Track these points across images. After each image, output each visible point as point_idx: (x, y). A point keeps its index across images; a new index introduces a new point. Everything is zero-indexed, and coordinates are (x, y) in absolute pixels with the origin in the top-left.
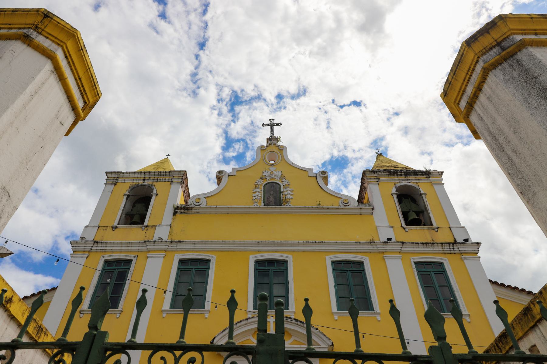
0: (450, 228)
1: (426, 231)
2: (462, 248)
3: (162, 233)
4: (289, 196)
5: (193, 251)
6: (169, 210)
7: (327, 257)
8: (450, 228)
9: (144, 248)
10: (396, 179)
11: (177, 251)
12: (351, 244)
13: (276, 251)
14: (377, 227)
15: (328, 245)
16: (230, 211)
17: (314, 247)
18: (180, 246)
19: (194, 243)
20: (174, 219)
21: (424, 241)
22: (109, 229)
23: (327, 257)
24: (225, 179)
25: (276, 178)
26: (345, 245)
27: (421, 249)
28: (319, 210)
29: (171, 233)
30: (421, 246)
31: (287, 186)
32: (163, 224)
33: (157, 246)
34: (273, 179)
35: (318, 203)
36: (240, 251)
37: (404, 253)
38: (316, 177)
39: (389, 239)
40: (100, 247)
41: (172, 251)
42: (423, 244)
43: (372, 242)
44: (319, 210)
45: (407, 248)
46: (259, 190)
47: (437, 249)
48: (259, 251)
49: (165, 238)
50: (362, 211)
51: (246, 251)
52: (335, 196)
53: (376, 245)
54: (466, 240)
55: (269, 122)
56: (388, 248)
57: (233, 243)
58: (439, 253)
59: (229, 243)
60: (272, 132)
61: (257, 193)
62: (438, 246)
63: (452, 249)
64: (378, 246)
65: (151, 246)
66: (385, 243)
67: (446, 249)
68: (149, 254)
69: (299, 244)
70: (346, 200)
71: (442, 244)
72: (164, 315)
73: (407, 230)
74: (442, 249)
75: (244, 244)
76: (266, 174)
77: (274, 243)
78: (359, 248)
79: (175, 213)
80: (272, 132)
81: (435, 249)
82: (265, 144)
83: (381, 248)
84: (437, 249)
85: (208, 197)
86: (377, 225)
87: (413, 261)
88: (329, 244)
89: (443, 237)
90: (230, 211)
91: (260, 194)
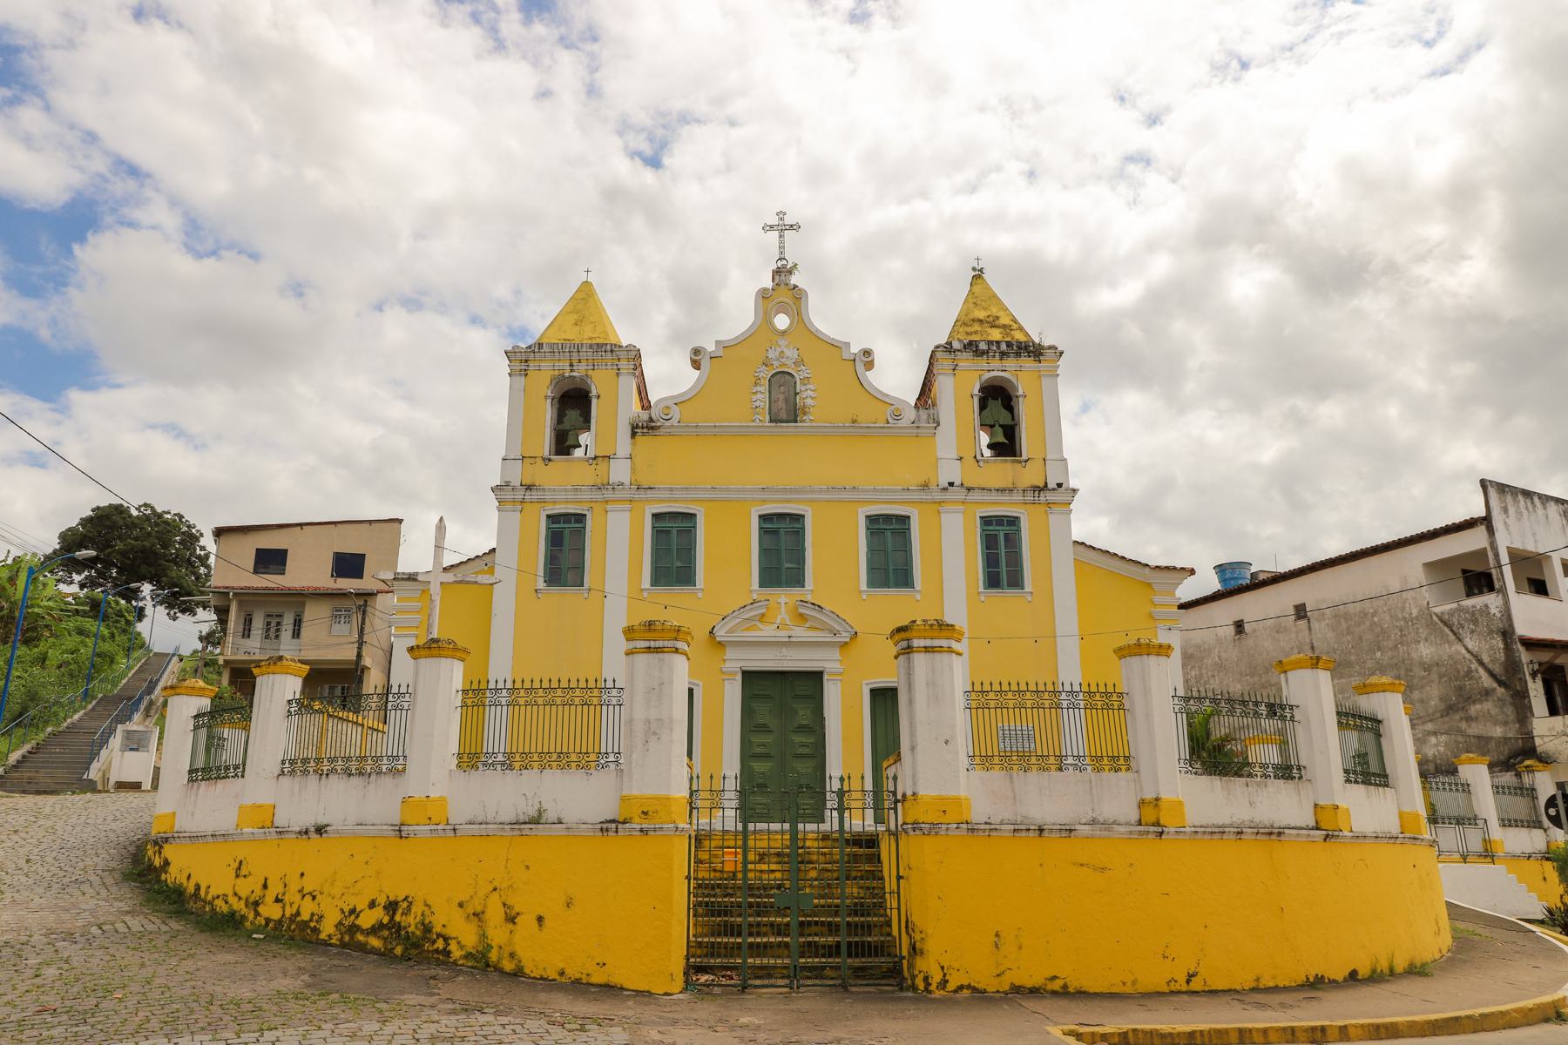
1: (1009, 465)
2: (1051, 497)
3: (620, 472)
4: (809, 402)
5: (669, 500)
6: (624, 431)
9: (597, 496)
11: (647, 500)
13: (788, 501)
16: (717, 432)
17: (843, 496)
18: (650, 494)
19: (671, 490)
20: (634, 444)
22: (539, 461)
24: (705, 363)
25: (789, 362)
27: (994, 497)
28: (855, 429)
29: (633, 470)
31: (805, 381)
32: (619, 454)
33: (618, 495)
34: (784, 365)
36: (738, 500)
39: (951, 484)
40: (535, 495)
41: (641, 500)
43: (925, 486)
44: (855, 429)
45: (975, 496)
46: (761, 389)
48: (764, 501)
49: (627, 481)
51: (745, 500)
52: (881, 400)
54: (1060, 485)
55: (774, 221)
57: (728, 490)
59: (721, 490)
60: (782, 247)
61: (759, 396)
65: (609, 495)
66: (945, 489)
67: (1029, 497)
68: (609, 507)
69: (821, 491)
72: (645, 594)
75: (743, 491)
76: (771, 355)
77: (785, 490)
79: (634, 434)
80: (782, 247)
82: (769, 284)
83: (938, 496)
85: (680, 402)
86: (939, 455)
88: (864, 491)
90: (717, 432)
91: (762, 399)
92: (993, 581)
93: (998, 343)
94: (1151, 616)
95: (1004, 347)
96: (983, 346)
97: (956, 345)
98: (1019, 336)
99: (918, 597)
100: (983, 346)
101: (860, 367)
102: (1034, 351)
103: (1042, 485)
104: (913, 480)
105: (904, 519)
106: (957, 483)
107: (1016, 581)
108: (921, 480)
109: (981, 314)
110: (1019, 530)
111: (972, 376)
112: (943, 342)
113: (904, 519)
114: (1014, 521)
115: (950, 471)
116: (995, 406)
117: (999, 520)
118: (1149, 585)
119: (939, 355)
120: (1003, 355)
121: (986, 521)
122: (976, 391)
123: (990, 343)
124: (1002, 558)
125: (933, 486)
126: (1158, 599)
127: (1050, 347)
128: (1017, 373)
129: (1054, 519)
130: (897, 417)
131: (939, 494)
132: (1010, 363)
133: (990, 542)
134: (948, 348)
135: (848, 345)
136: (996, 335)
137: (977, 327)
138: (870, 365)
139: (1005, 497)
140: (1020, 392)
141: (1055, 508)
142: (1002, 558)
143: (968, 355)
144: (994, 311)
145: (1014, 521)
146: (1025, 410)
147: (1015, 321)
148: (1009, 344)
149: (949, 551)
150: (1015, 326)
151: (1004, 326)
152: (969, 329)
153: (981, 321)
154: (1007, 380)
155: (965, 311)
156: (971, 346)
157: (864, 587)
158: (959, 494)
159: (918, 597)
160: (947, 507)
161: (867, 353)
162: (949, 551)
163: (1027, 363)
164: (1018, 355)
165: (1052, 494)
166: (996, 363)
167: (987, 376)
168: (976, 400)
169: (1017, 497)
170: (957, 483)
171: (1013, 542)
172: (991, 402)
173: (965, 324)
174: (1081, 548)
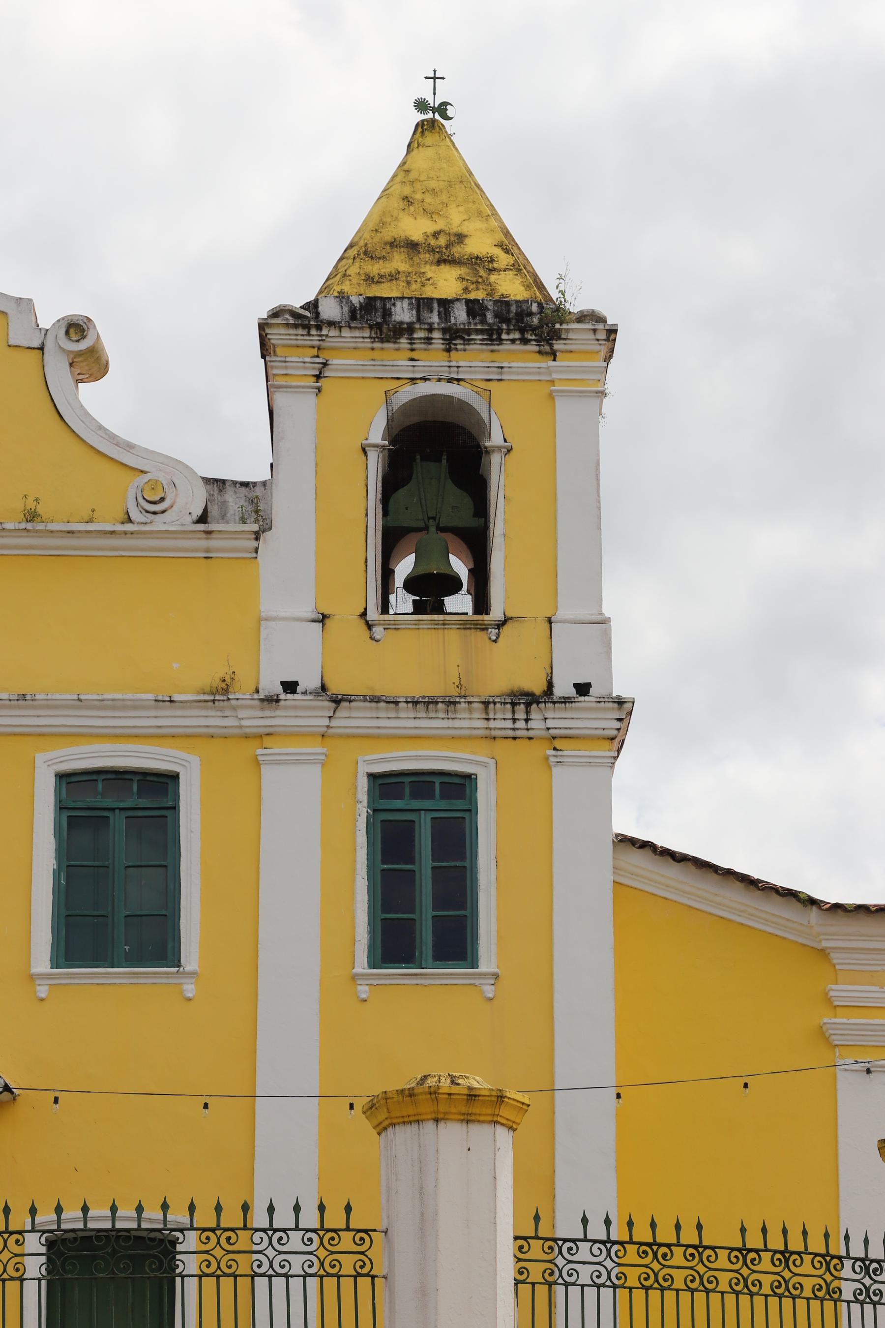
0: (550, 622)
2: (556, 719)
7: (40, 758)
8: (550, 622)
10: (397, 358)
12: (136, 706)
14: (260, 620)
15: (48, 707)
21: (417, 694)
23: (40, 758)
26: (113, 708)
27: (408, 721)
30: (406, 711)
35: (31, 504)
37: (341, 736)
38: (41, 348)
39: (290, 687)
42: (415, 703)
43: (221, 693)
45: (353, 719)
47: (465, 724)
50: (213, 543)
53: (234, 708)
54: (583, 689)
56: (279, 719)
58: (470, 738)
62: (470, 711)
63: (521, 724)
64: (241, 714)
67: (501, 722)
70: (154, 484)
71: (486, 704)
73: (378, 631)
74: (482, 724)
78: (169, 720)
81: (457, 724)
83: (253, 719)
84: (465, 724)
87: (364, 769)
88: (51, 705)
89: (509, 665)
92: (394, 945)
93: (445, 304)
94: (822, 1035)
95: (460, 315)
96: (403, 314)
97: (330, 310)
98: (511, 287)
99: (190, 989)
100: (403, 314)
101: (58, 370)
102: (536, 324)
103: (537, 687)
104: (191, 675)
105: (163, 784)
106: (309, 681)
107: (456, 944)
108: (211, 676)
109: (416, 228)
110: (472, 810)
111: (369, 395)
112: (297, 302)
113: (163, 784)
114: (460, 786)
115: (293, 653)
116: (432, 482)
117: (421, 783)
118: (823, 953)
119: (276, 335)
120: (454, 337)
121: (384, 785)
122: (377, 435)
123: (422, 304)
124: (422, 880)
125: (242, 693)
126: (841, 991)
127: (582, 317)
128: (499, 389)
129: (568, 780)
130: (156, 504)
131: (255, 711)
132: (473, 360)
133: (391, 843)
134: (306, 319)
135: (25, 305)
136: (446, 283)
137: (399, 262)
138: (91, 364)
139: (437, 722)
140: (496, 439)
141: (570, 751)
142: (422, 880)
143: (357, 336)
144: (455, 218)
145: (460, 786)
146: (504, 481)
147: (508, 245)
148: (474, 308)
149: (277, 862)
150: (504, 260)
151: (474, 261)
152: (375, 268)
153: (412, 246)
154: (462, 406)
155: (378, 221)
156: (372, 317)
157: (41, 958)
158: (317, 716)
159: (190, 989)
160: (277, 748)
161: (76, 328)
162: (277, 862)
163: (519, 359)
164: (493, 336)
165: (569, 714)
166: (433, 359)
167: (408, 393)
168: (375, 464)
169: (470, 721)
170: (309, 681)
171: (456, 840)
172: (422, 470)
173: (368, 254)
174: (638, 859)
